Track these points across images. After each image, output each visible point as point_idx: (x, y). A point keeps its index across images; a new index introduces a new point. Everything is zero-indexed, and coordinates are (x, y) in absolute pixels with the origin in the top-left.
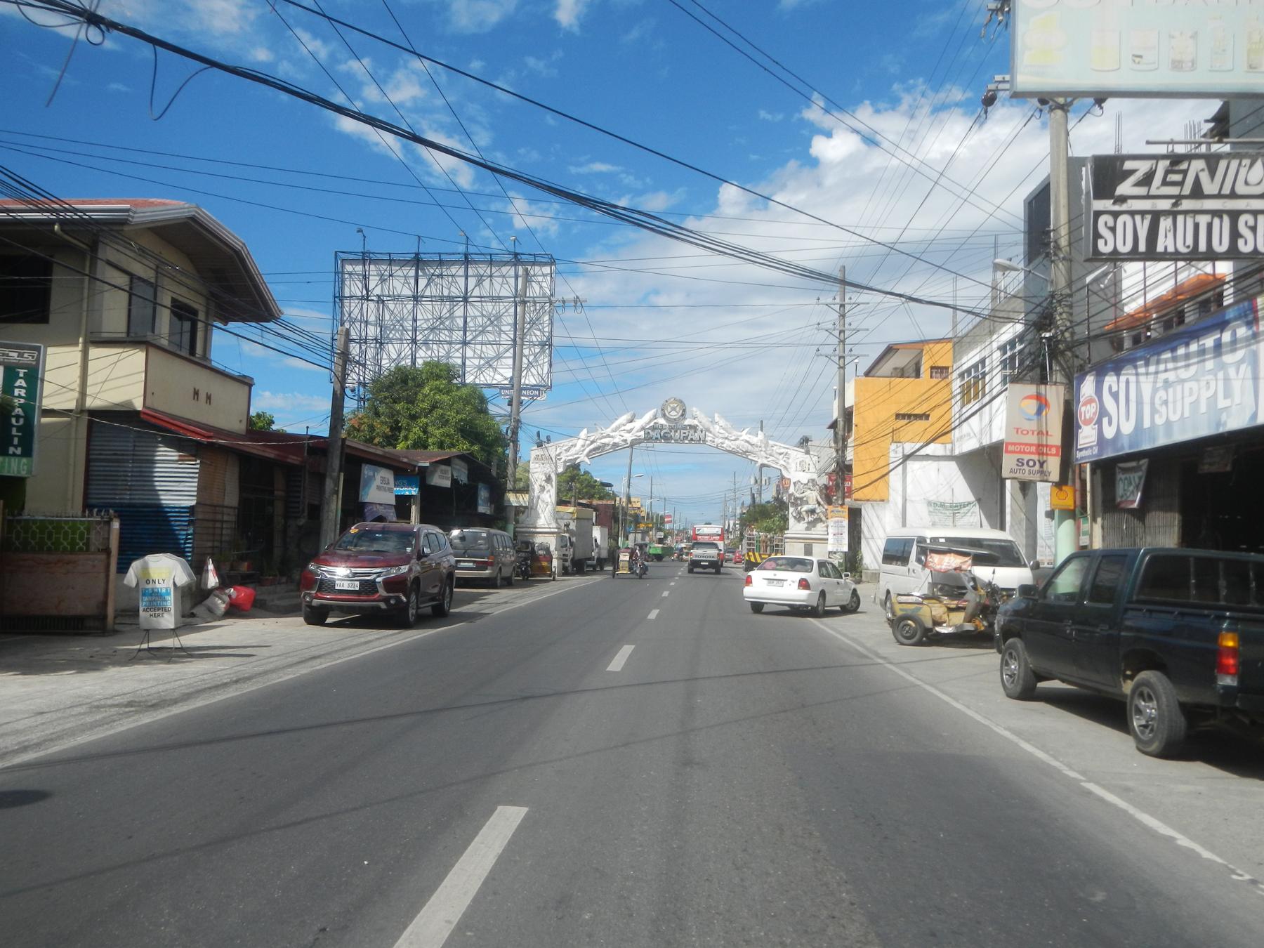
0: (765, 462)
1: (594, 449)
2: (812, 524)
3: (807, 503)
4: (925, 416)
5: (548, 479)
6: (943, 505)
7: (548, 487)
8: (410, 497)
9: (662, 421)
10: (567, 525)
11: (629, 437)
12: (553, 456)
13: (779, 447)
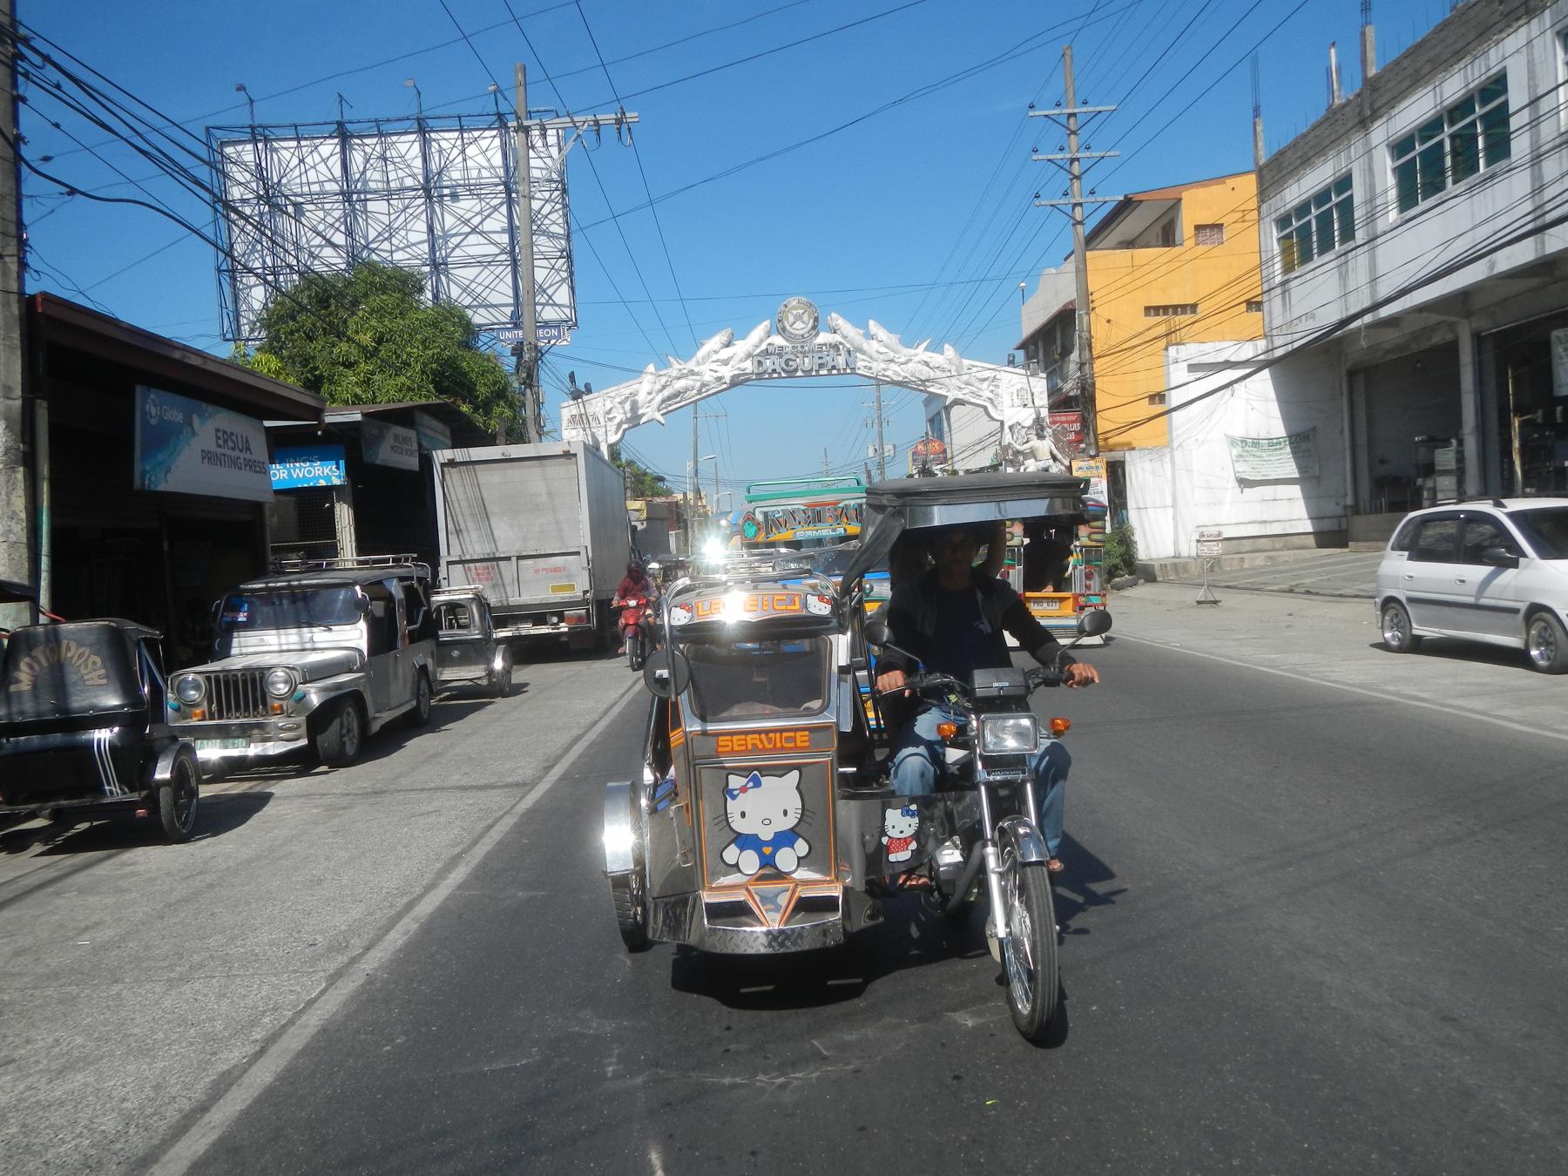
1: (669, 398)
4: (1194, 307)
6: (1256, 443)
8: (328, 491)
9: (778, 340)
11: (727, 373)
13: (980, 369)
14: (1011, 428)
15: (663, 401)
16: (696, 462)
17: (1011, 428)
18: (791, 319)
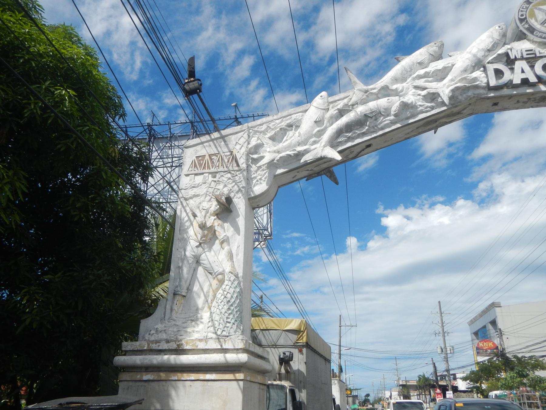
1: (349, 127)
5: (226, 209)
7: (224, 230)
10: (285, 361)
12: (241, 153)
15: (339, 132)
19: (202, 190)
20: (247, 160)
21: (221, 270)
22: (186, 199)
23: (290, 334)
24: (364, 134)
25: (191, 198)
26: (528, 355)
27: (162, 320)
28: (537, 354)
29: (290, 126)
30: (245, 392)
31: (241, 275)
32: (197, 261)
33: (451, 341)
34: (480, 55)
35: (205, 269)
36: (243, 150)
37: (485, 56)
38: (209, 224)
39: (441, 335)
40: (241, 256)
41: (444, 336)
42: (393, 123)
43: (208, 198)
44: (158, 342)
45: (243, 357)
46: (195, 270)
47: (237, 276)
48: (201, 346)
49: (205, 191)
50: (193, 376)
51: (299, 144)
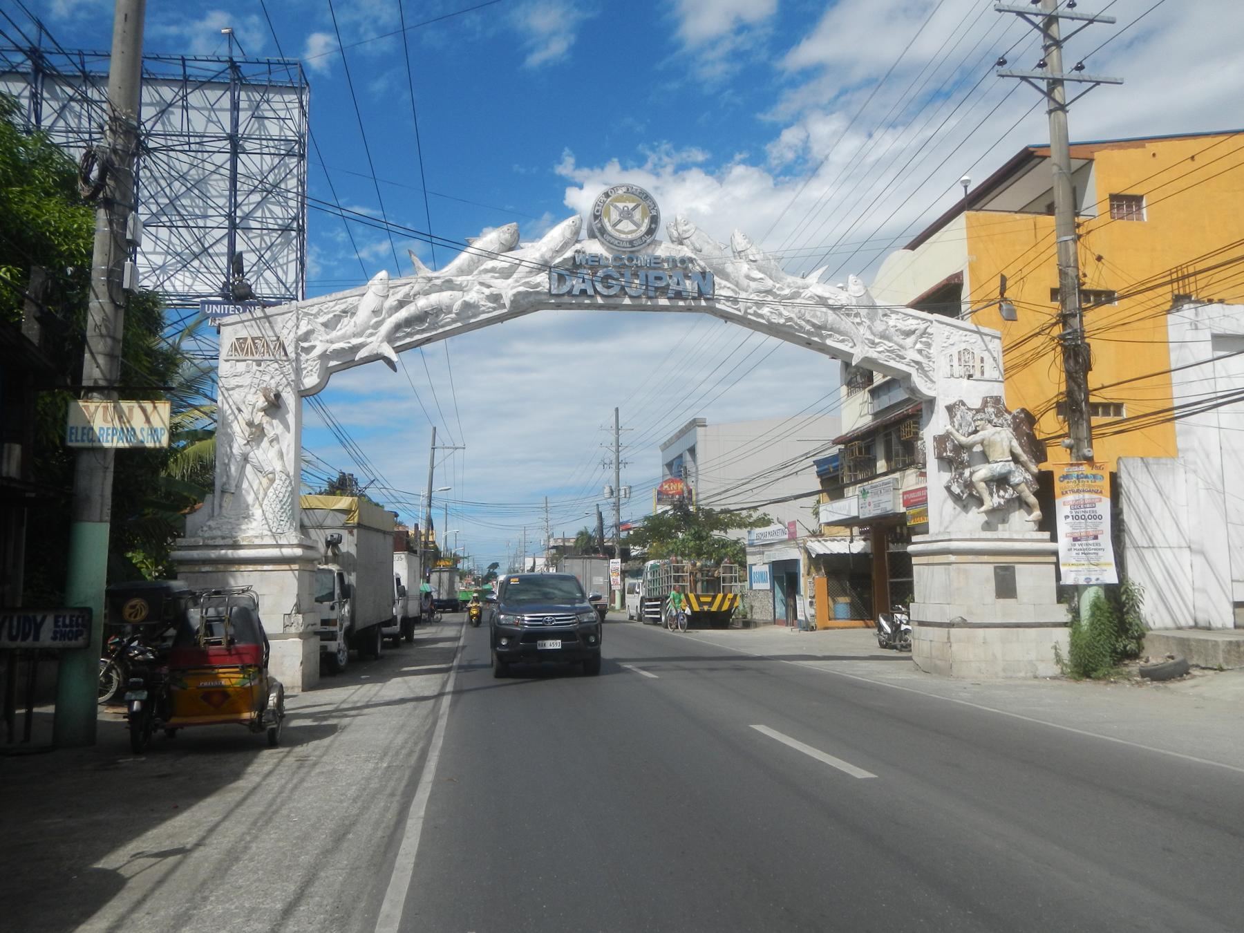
0: (872, 354)
1: (408, 322)
2: (998, 515)
3: (985, 458)
5: (274, 406)
7: (273, 427)
9: (595, 248)
10: (333, 543)
11: (508, 289)
12: (289, 341)
14: (950, 409)
15: (398, 327)
16: (431, 491)
17: (950, 409)
18: (615, 216)
19: (246, 380)
20: (296, 348)
21: (271, 469)
22: (227, 390)
23: (339, 515)
24: (423, 331)
25: (233, 389)
26: (718, 509)
27: (211, 516)
28: (732, 507)
29: (345, 312)
30: (300, 580)
31: (292, 474)
32: (245, 459)
33: (629, 475)
34: (547, 256)
35: (254, 466)
36: (292, 335)
37: (553, 258)
38: (256, 422)
39: (613, 466)
40: (292, 455)
41: (618, 468)
42: (454, 321)
43: (253, 390)
44: (213, 538)
45: (298, 552)
46: (243, 467)
47: (288, 475)
48: (257, 542)
49: (249, 382)
50: (251, 568)
51: (354, 335)
